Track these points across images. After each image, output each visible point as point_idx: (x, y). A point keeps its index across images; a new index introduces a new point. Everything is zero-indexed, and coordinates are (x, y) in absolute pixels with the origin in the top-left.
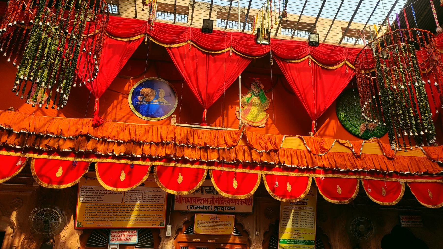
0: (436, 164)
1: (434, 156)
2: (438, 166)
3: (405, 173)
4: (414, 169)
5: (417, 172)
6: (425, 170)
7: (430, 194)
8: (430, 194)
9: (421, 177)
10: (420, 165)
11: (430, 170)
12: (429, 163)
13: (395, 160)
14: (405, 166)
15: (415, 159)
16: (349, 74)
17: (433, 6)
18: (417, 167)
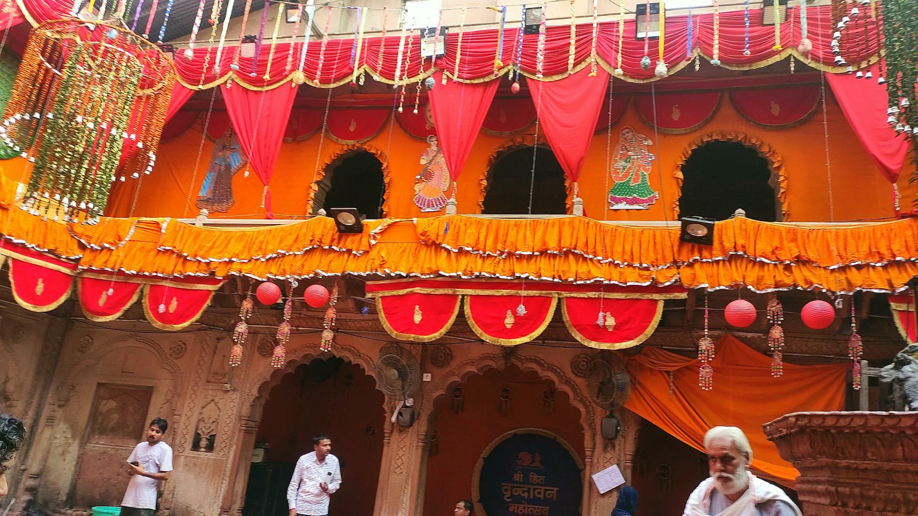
0: (75, 242)
1: (78, 230)
2: (75, 247)
3: (16, 241)
4: (35, 240)
5: (38, 246)
6: (52, 247)
7: (40, 288)
8: (40, 288)
9: (39, 255)
10: (49, 235)
11: (61, 250)
12: (66, 237)
13: (11, 213)
14: (21, 229)
15: (46, 225)
16: (8, 15)
17: (200, 13)
18: (42, 238)
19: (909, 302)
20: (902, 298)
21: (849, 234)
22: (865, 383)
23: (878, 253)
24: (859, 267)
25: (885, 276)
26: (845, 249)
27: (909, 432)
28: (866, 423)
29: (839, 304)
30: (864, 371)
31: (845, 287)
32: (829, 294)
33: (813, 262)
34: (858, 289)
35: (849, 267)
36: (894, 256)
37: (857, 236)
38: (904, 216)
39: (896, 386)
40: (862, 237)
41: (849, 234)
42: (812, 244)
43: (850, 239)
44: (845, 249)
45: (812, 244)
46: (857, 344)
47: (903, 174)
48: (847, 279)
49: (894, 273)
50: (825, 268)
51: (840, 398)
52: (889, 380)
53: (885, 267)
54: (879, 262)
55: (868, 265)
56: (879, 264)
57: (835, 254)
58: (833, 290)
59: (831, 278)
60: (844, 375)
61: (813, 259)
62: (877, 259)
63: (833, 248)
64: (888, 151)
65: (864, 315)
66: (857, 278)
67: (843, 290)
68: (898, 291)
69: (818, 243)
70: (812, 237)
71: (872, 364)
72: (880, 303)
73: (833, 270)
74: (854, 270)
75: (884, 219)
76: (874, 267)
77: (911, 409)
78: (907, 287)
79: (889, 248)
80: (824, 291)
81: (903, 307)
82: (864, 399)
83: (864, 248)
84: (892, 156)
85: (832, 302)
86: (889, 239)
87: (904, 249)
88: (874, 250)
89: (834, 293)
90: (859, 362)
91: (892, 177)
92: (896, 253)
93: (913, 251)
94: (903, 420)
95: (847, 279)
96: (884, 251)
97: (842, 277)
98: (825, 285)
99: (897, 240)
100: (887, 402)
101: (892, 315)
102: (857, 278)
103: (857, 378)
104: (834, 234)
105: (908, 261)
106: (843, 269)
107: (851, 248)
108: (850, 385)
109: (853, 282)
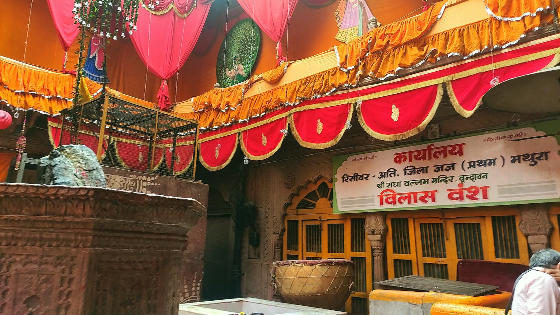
19: (59, 123)
20: (56, 119)
21: (33, 73)
22: (23, 167)
23: (48, 90)
24: (34, 96)
25: (49, 104)
26: (28, 82)
27: (52, 197)
28: (26, 191)
29: (17, 116)
30: (23, 159)
31: (23, 106)
32: (11, 108)
33: (4, 85)
34: (31, 109)
35: (28, 94)
36: (57, 94)
37: (38, 76)
38: (67, 72)
39: (48, 170)
40: (40, 78)
41: (33, 73)
42: (6, 73)
43: (32, 77)
44: (28, 82)
45: (6, 73)
46: (23, 142)
47: (71, 48)
48: (25, 101)
49: (54, 104)
50: (12, 91)
51: (4, 174)
52: (44, 165)
53: (50, 99)
54: (47, 95)
55: (40, 96)
56: (47, 97)
57: (21, 83)
58: (15, 106)
59: (15, 98)
60: (10, 161)
61: (5, 83)
62: (46, 93)
63: (21, 80)
64: (66, 31)
65: (31, 126)
66: (32, 102)
67: (21, 107)
68: (54, 115)
69: (11, 73)
70: (7, 68)
71: (29, 156)
72: (42, 120)
73: (17, 94)
74: (31, 97)
75: (55, 71)
76: (43, 98)
77: (54, 184)
78: (60, 114)
79: (55, 89)
80: (8, 105)
81: (55, 125)
82: (20, 176)
83: (40, 85)
84: (68, 35)
85: (12, 114)
86: (56, 83)
87: (63, 92)
88: (46, 87)
89: (14, 108)
90: (22, 154)
91: (66, 48)
92: (58, 93)
93: (67, 94)
94: (50, 190)
95: (25, 101)
96: (51, 89)
97: (23, 99)
98: (10, 102)
99: (60, 85)
100: (40, 179)
101: (47, 128)
102: (32, 102)
103: (18, 163)
104: (23, 71)
105: (64, 99)
106: (24, 94)
107: (32, 82)
108: (13, 167)
109: (29, 104)
